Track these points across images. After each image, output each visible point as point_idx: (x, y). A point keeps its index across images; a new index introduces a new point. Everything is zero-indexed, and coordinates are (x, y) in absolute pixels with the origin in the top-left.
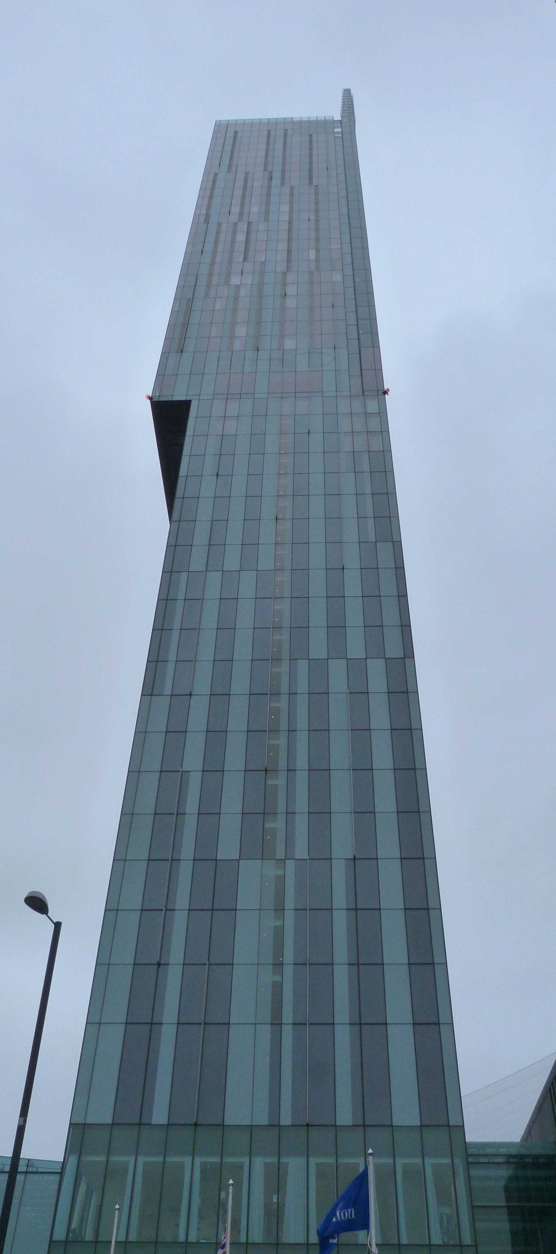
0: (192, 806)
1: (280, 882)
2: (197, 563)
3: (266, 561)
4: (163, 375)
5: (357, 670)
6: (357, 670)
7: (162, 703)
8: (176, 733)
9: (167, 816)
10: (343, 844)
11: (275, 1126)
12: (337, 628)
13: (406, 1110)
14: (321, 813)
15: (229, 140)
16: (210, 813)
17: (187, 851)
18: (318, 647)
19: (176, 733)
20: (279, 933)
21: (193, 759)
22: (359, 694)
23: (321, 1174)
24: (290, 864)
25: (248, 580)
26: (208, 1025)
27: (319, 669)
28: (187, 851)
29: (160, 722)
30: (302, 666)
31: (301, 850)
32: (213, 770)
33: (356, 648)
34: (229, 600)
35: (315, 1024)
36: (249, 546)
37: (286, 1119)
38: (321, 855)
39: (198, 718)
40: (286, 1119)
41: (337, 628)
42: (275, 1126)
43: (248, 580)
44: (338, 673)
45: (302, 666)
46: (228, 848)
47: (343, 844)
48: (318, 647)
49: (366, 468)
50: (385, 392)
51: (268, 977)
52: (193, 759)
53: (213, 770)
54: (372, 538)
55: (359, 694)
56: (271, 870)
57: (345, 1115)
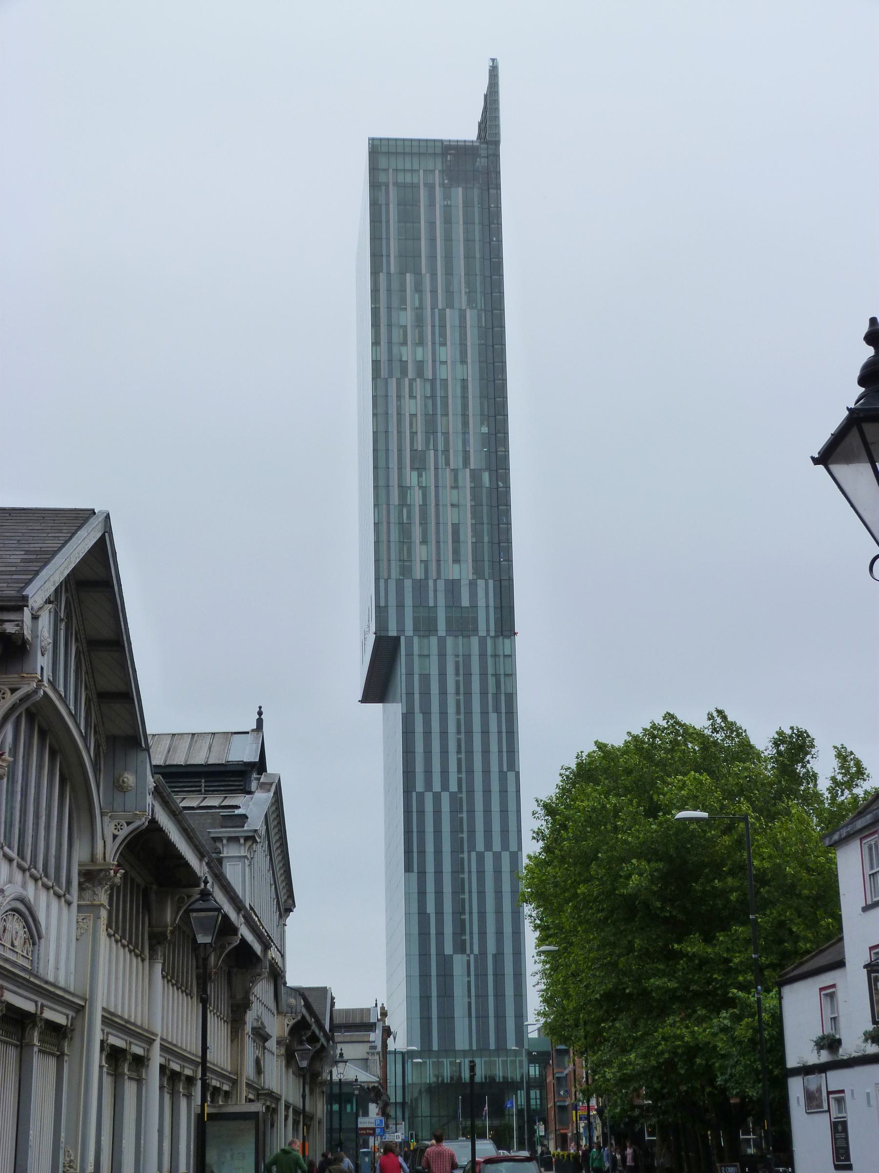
0: (433, 931)
1: (469, 962)
2: (420, 786)
3: (453, 787)
4: (381, 612)
5: (497, 857)
6: (497, 857)
7: (414, 876)
8: (422, 893)
9: (424, 934)
10: (491, 949)
11: (471, 1050)
12: (488, 832)
13: (512, 1045)
14: (483, 933)
15: (381, 152)
16: (440, 934)
17: (433, 951)
18: (480, 846)
19: (422, 893)
20: (469, 982)
21: (431, 908)
22: (498, 872)
23: (485, 1062)
24: (472, 956)
25: (445, 798)
26: (447, 1019)
27: (481, 857)
28: (433, 951)
29: (415, 889)
30: (473, 854)
31: (476, 950)
32: (440, 913)
33: (497, 847)
34: (437, 812)
35: (482, 1017)
36: (445, 772)
37: (474, 1048)
38: (483, 953)
39: (430, 887)
40: (474, 1048)
41: (488, 832)
42: (471, 1050)
43: (445, 798)
44: (489, 857)
45: (473, 854)
46: (448, 949)
47: (491, 949)
48: (480, 846)
49: (503, 711)
50: (515, 634)
51: (466, 1000)
52: (431, 908)
53: (440, 913)
54: (505, 769)
55: (498, 872)
56: (465, 957)
57: (492, 1046)
